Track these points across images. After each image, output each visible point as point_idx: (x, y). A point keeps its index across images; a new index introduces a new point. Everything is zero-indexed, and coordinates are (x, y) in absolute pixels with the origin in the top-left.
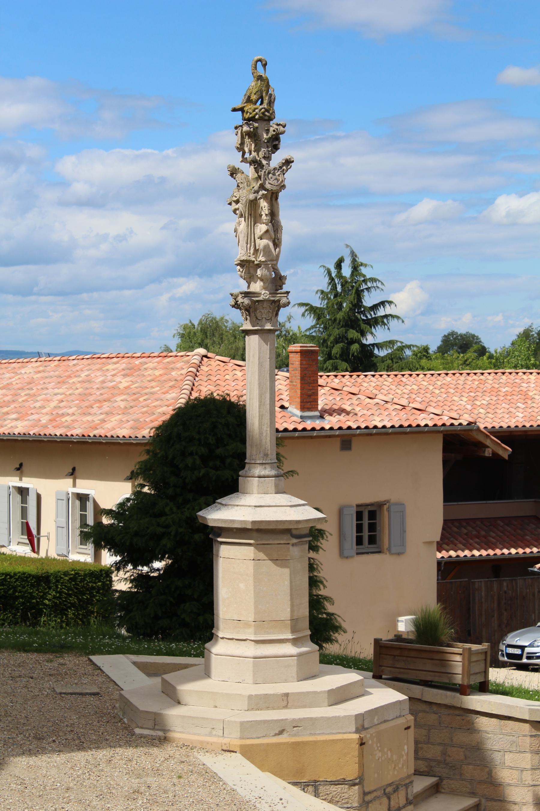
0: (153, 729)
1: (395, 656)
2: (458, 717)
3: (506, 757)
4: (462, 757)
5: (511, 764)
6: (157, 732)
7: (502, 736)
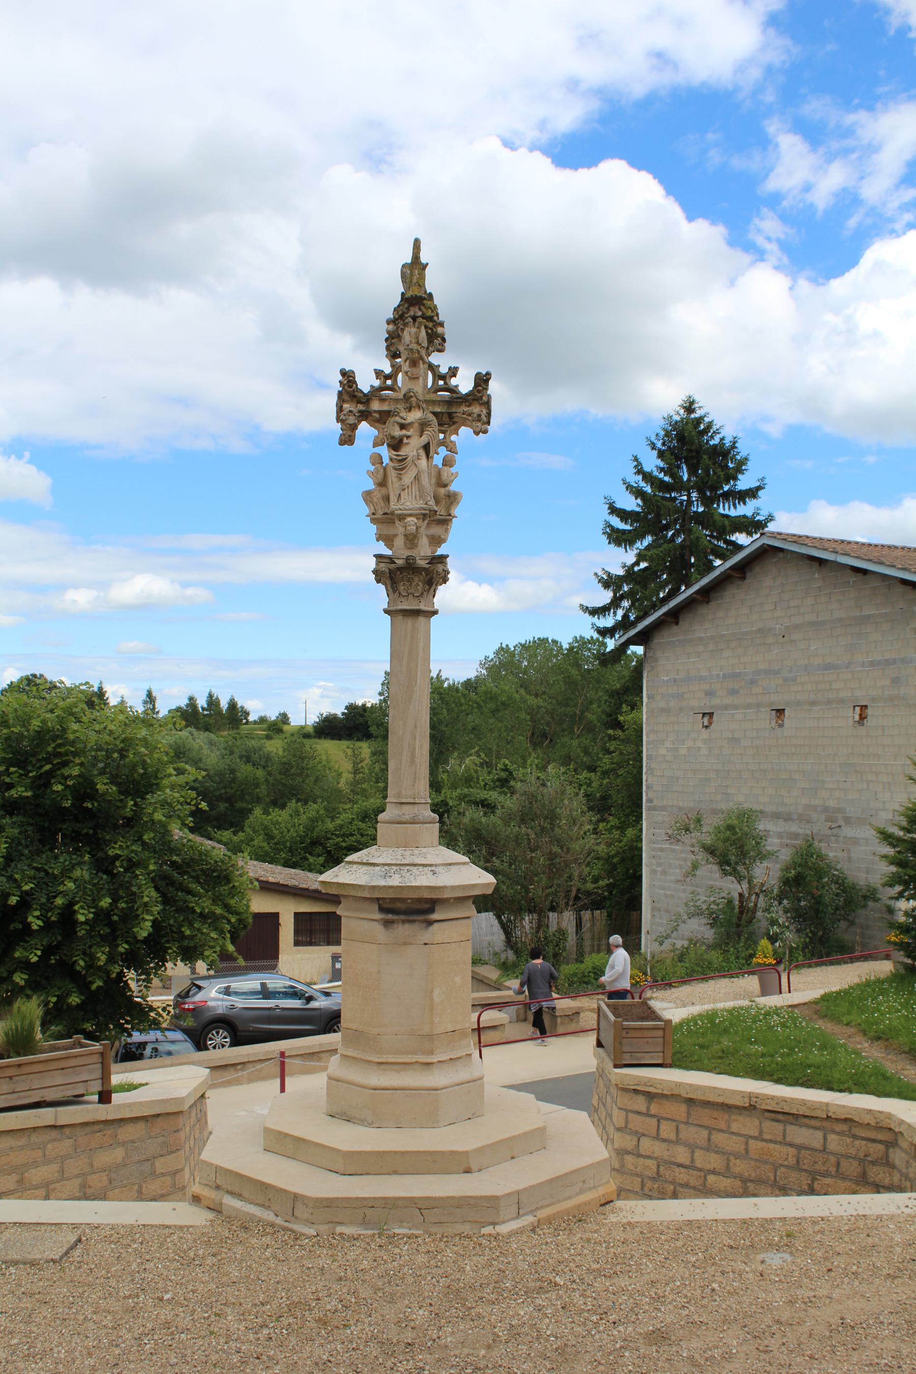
0: (518, 1216)
1: (11, 1078)
2: (98, 1134)
3: (157, 1164)
4: (106, 1183)
5: (162, 1171)
6: (524, 1218)
7: (149, 1141)
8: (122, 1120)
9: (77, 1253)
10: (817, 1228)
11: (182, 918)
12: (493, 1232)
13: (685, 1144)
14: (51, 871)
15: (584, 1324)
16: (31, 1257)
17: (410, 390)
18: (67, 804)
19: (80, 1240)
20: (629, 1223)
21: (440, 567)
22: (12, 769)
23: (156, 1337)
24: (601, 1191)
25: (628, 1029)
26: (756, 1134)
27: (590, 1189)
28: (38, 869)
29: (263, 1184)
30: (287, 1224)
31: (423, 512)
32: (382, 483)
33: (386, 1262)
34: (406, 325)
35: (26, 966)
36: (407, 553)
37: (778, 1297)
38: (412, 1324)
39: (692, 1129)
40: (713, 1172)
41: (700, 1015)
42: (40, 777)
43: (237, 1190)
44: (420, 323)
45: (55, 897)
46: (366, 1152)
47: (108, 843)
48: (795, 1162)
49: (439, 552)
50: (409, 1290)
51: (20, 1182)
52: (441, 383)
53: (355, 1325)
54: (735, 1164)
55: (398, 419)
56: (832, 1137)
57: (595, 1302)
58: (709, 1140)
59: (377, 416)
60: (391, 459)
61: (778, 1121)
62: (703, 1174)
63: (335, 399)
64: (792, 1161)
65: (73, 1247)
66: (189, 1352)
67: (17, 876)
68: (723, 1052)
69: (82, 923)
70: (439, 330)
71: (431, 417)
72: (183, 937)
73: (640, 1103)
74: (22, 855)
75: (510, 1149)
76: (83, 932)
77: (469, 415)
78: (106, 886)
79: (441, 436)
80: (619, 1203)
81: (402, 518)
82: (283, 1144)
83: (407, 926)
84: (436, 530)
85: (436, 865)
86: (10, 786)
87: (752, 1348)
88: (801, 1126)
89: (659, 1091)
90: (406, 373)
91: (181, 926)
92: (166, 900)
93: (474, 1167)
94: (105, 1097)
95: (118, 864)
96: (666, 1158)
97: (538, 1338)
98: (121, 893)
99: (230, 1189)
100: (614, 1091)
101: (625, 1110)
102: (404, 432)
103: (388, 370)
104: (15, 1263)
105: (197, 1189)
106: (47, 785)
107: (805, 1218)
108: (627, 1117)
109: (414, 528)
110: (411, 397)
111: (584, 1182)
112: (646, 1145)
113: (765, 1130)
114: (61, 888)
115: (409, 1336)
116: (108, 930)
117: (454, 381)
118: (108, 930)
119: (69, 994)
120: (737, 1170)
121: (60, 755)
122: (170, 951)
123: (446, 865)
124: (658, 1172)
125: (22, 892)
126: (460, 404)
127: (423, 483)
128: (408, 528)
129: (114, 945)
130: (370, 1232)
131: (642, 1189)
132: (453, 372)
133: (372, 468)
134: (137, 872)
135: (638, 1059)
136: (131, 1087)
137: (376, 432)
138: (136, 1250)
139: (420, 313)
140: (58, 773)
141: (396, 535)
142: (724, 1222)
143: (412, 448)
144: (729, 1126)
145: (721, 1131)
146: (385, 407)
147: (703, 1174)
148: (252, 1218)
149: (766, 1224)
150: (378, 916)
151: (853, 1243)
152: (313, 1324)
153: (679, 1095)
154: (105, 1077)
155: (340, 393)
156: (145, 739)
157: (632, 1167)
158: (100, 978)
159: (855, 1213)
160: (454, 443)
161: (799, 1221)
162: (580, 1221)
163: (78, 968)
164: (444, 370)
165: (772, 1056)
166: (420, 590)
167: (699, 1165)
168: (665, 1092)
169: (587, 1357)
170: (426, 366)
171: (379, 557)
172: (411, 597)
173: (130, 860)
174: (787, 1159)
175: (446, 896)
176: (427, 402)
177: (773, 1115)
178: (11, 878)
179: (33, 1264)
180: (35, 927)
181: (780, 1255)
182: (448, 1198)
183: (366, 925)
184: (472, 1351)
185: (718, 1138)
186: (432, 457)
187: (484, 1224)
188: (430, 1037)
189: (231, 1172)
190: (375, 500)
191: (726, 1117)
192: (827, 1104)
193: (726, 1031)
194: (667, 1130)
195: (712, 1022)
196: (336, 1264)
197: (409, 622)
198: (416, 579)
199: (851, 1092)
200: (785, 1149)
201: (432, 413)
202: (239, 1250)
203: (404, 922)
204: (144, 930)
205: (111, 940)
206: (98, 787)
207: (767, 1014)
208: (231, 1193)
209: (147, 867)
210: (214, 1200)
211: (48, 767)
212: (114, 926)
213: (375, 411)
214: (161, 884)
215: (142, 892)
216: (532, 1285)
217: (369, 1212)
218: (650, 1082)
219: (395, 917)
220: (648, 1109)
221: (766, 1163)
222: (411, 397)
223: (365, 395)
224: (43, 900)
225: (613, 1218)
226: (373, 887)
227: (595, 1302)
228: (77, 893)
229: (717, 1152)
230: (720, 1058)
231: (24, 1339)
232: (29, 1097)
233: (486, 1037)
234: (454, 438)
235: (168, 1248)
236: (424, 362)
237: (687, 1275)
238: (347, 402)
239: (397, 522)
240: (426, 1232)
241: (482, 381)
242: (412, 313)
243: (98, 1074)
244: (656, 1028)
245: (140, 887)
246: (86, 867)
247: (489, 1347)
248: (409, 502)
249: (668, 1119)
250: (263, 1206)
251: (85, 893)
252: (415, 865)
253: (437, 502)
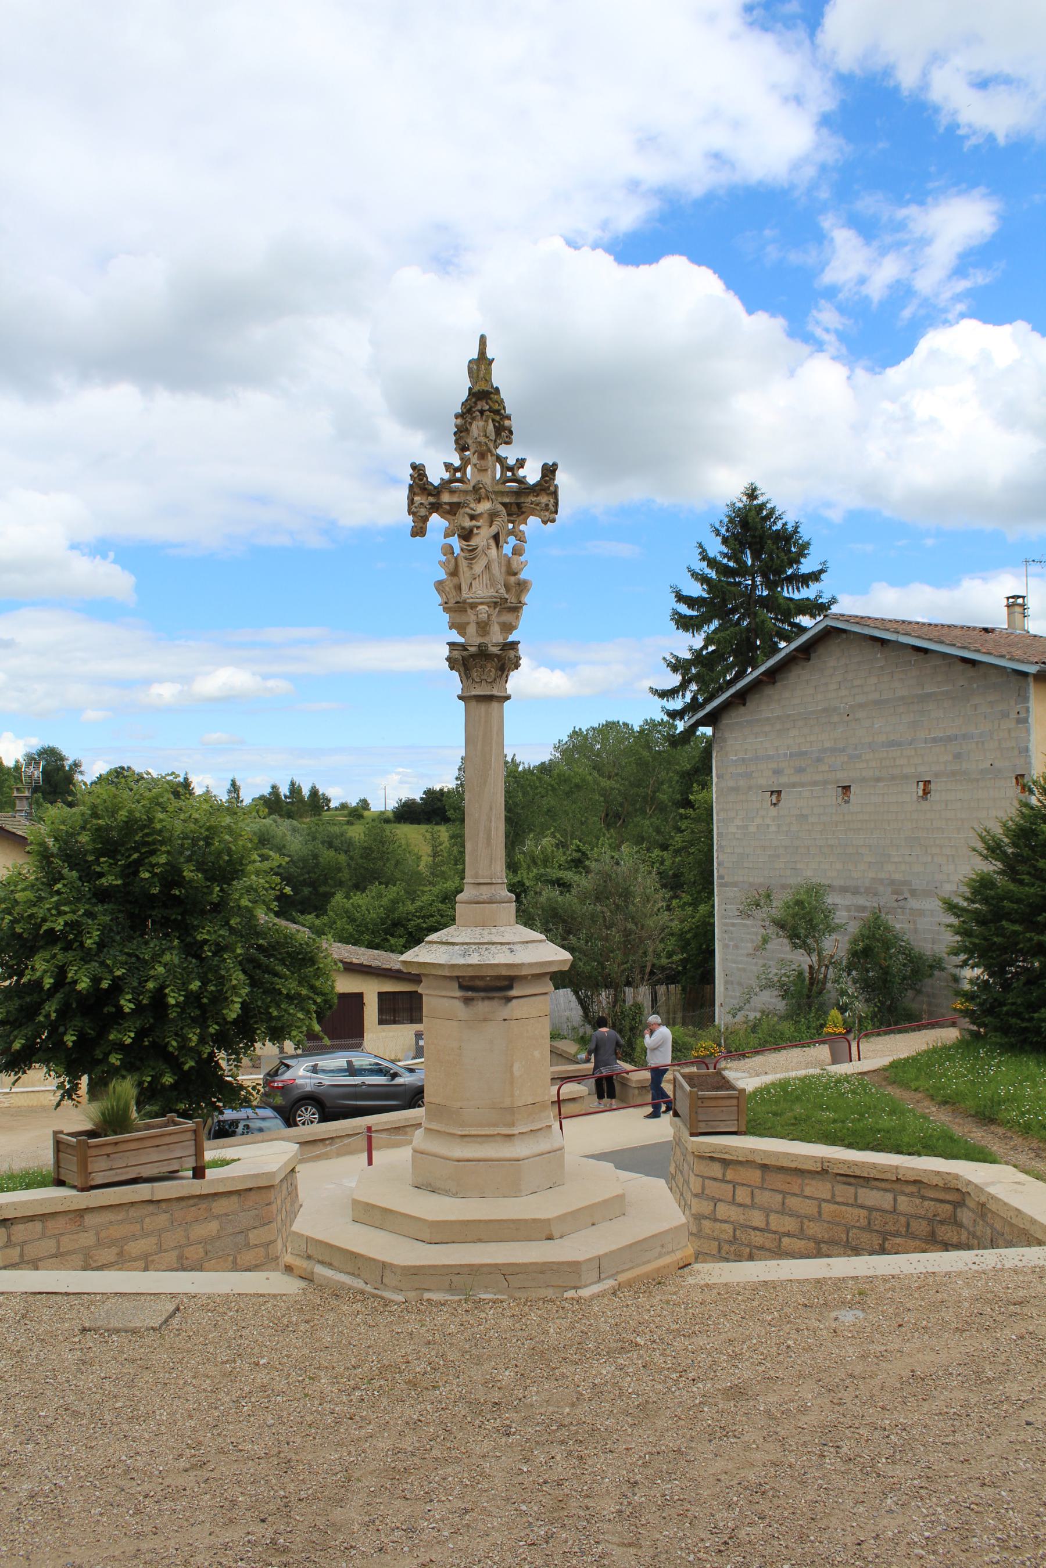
0: (600, 1280)
1: (108, 1155)
3: (250, 1236)
4: (202, 1254)
8: (215, 1194)
9: (175, 1321)
10: (888, 1286)
11: (269, 999)
12: (576, 1296)
13: (761, 1208)
14: (141, 956)
15: (665, 1382)
16: (132, 1325)
17: (479, 482)
18: (155, 891)
19: (178, 1309)
20: (707, 1285)
21: (512, 654)
22: (102, 860)
23: (253, 1400)
24: (679, 1255)
25: (702, 1099)
26: (829, 1198)
27: (668, 1253)
28: (129, 955)
29: (352, 1253)
30: (376, 1291)
32: (454, 573)
33: (472, 1326)
34: (474, 419)
35: (120, 1047)
36: (480, 640)
37: (851, 1352)
38: (499, 1384)
39: (767, 1193)
40: (788, 1234)
41: (773, 1084)
42: (129, 865)
43: (327, 1260)
44: (488, 417)
45: (146, 981)
46: (451, 1222)
47: (195, 928)
48: (866, 1223)
49: (511, 639)
50: (495, 1352)
51: (120, 1254)
52: (509, 474)
53: (444, 1386)
54: (808, 1226)
55: (467, 510)
56: (901, 1199)
57: (674, 1361)
58: (783, 1204)
59: (448, 507)
60: (462, 550)
61: (849, 1184)
62: (777, 1236)
63: (406, 492)
64: (863, 1222)
65: (172, 1315)
66: (285, 1414)
67: (108, 962)
68: (796, 1119)
69: (173, 1006)
70: (507, 423)
71: (500, 508)
72: (271, 1018)
73: (716, 1170)
74: (114, 941)
75: (591, 1216)
76: (175, 1014)
77: (537, 505)
78: (196, 970)
79: (511, 526)
80: (697, 1266)
81: (473, 606)
82: (370, 1214)
83: (486, 1003)
84: (507, 618)
85: (513, 943)
86: (101, 875)
87: (827, 1401)
88: (872, 1189)
89: (735, 1158)
90: (475, 465)
91: (269, 1007)
92: (254, 983)
93: (556, 1234)
94: (199, 1173)
95: (206, 948)
96: (742, 1222)
97: (620, 1396)
98: (210, 976)
99: (320, 1258)
100: (690, 1158)
101: (702, 1177)
102: (474, 523)
103: (457, 463)
104: (117, 1331)
105: (288, 1259)
106: (136, 873)
107: (877, 1277)
108: (703, 1184)
111: (663, 1246)
112: (723, 1210)
113: (837, 1193)
114: (152, 973)
115: (496, 1396)
116: (198, 1012)
117: (521, 473)
118: (198, 1012)
119: (162, 1075)
120: (810, 1232)
121: (147, 844)
122: (258, 1032)
123: (523, 943)
124: (734, 1236)
125: (114, 977)
126: (528, 494)
129: (204, 1027)
130: (457, 1298)
131: (719, 1252)
132: (521, 463)
133: (444, 558)
134: (225, 956)
135: (713, 1127)
136: (224, 1163)
137: (446, 523)
138: (231, 1317)
139: (487, 407)
140: (146, 861)
141: (468, 623)
142: (798, 1281)
143: (482, 538)
144: (802, 1190)
145: (795, 1195)
146: (455, 499)
147: (777, 1236)
148: (343, 1286)
149: (839, 1283)
150: (459, 994)
151: (923, 1299)
152: (403, 1386)
153: (754, 1162)
154: (199, 1153)
155: (411, 486)
156: (229, 826)
157: (709, 1231)
158: (192, 1058)
159: (924, 1271)
160: (523, 532)
161: (870, 1279)
162: (659, 1283)
163: (171, 1049)
164: (511, 462)
165: (843, 1122)
167: (774, 1229)
168: (740, 1159)
169: (668, 1413)
170: (494, 458)
171: (450, 644)
173: (217, 944)
174: (858, 1221)
175: (524, 973)
176: (496, 493)
177: (844, 1178)
178: (103, 964)
179: (134, 1331)
180: (127, 1010)
181: (852, 1312)
182: (531, 1264)
183: (446, 1002)
184: (556, 1409)
185: (792, 1202)
186: (502, 547)
187: (566, 1289)
188: (511, 1110)
189: (321, 1242)
190: (447, 589)
191: (799, 1181)
192: (897, 1167)
193: (798, 1099)
194: (743, 1195)
195: (785, 1091)
196: (425, 1328)
197: (483, 707)
198: (489, 665)
199: (919, 1155)
200: (857, 1211)
201: (502, 503)
202: (331, 1316)
203: (483, 999)
204: (233, 1012)
205: (202, 1021)
206: (185, 874)
207: (838, 1081)
208: (322, 1263)
209: (234, 951)
210: (305, 1269)
211: (135, 856)
212: (203, 1008)
213: (445, 503)
214: (249, 967)
215: (231, 975)
216: (613, 1345)
217: (455, 1278)
218: (726, 1149)
219: (475, 994)
220: (724, 1175)
221: (838, 1224)
223: (435, 488)
224: (135, 984)
225: (691, 1280)
226: (453, 966)
227: (674, 1361)
228: (167, 977)
229: (791, 1216)
230: (793, 1124)
231: (128, 1403)
232: (127, 1173)
233: (566, 1109)
234: (522, 527)
235: (262, 1316)
236: (492, 455)
237: (763, 1334)
238: (418, 495)
239: (469, 610)
240: (511, 1297)
241: (549, 471)
242: (479, 407)
243: (192, 1151)
244: (730, 1097)
245: (228, 970)
246: (175, 952)
247: (573, 1405)
248: (480, 591)
249: (743, 1185)
250: (353, 1274)
251: (175, 977)
252: (493, 944)
253: (508, 590)
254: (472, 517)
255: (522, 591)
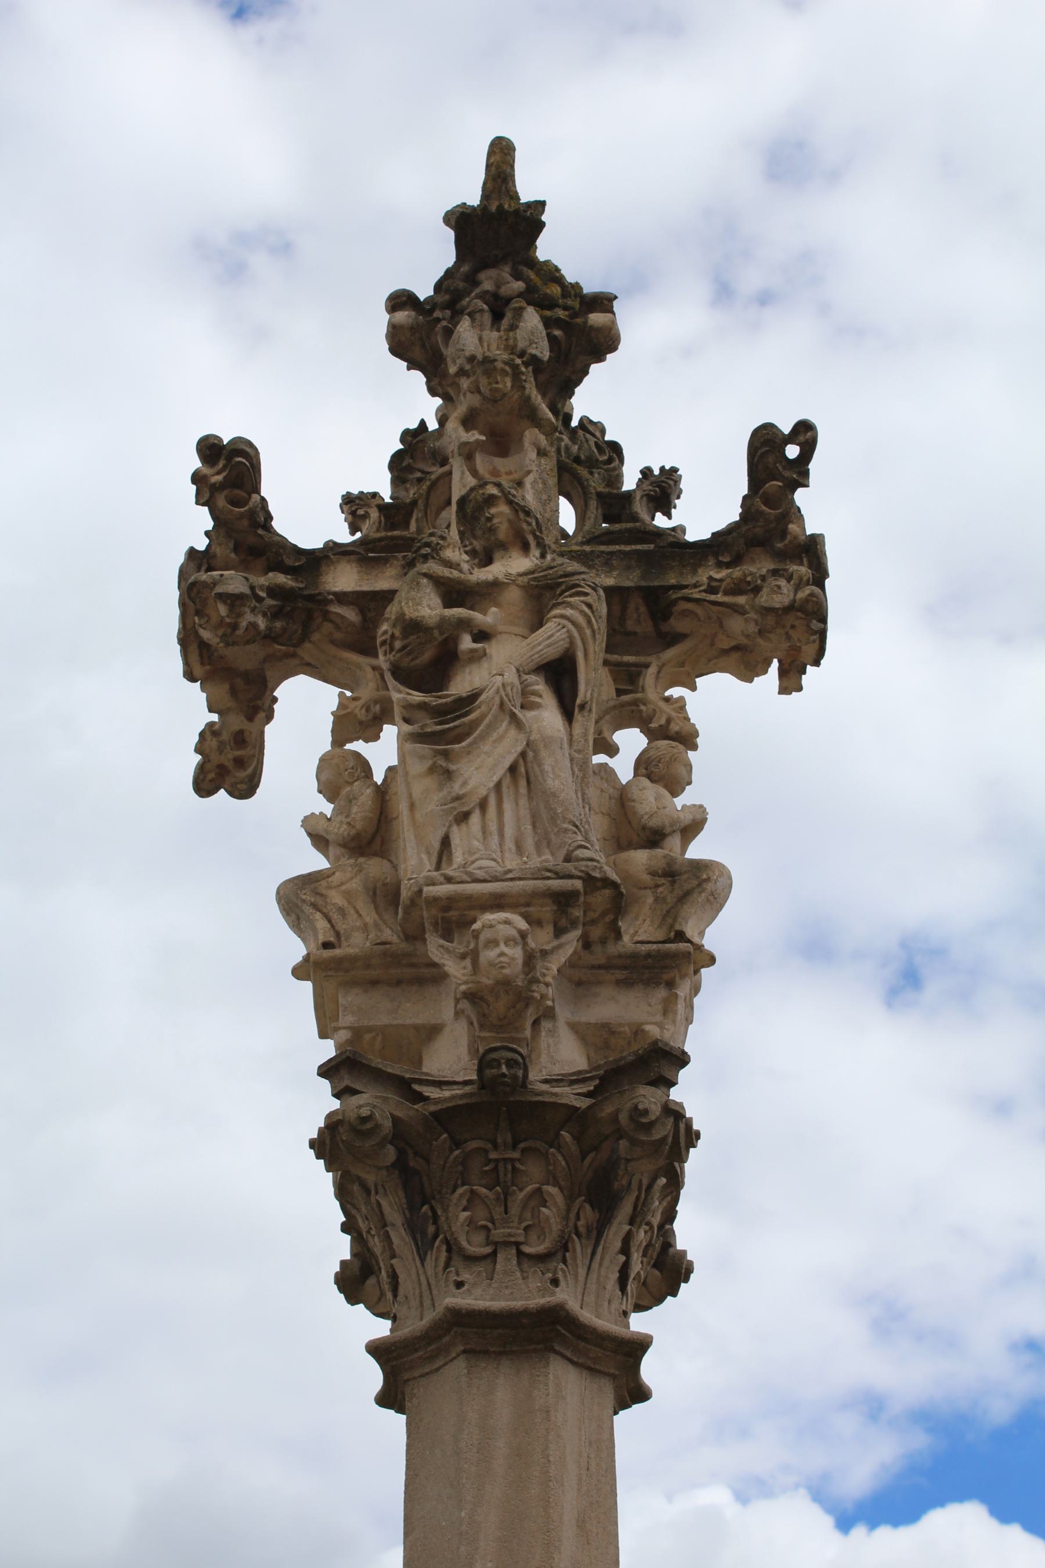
31: (556, 884)
55: (433, 567)
59: (350, 614)
81: (454, 918)
109: (516, 953)
110: (491, 500)
127: (552, 783)
128: (489, 955)
139: (519, 286)
166: (555, 1225)
172: (506, 1260)
190: (337, 898)
198: (533, 1171)
213: (342, 598)
222: (491, 500)
241: (778, 460)
254: (455, 593)
255: (684, 897)
